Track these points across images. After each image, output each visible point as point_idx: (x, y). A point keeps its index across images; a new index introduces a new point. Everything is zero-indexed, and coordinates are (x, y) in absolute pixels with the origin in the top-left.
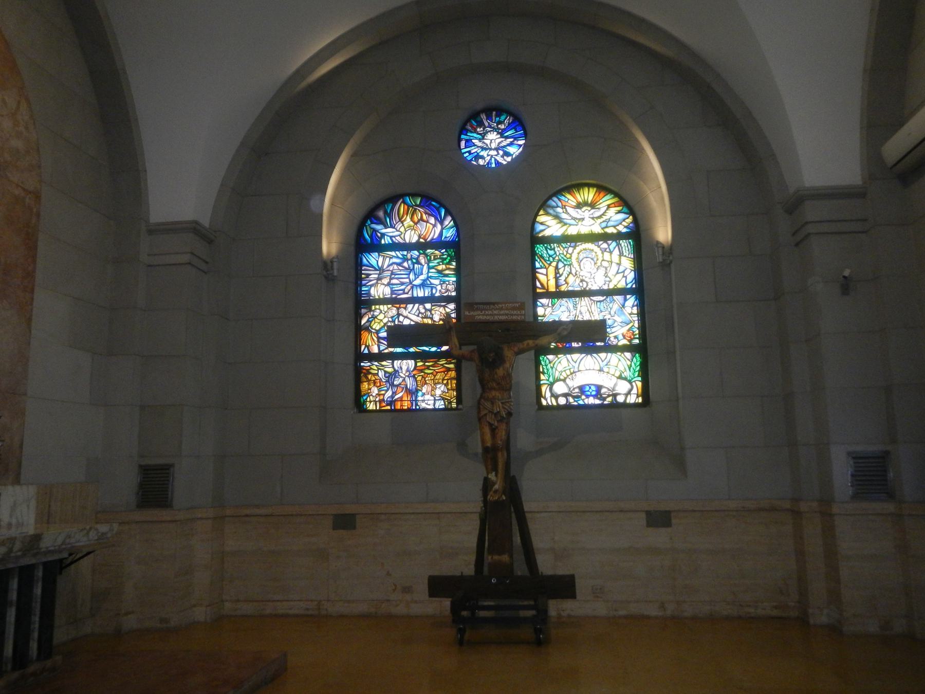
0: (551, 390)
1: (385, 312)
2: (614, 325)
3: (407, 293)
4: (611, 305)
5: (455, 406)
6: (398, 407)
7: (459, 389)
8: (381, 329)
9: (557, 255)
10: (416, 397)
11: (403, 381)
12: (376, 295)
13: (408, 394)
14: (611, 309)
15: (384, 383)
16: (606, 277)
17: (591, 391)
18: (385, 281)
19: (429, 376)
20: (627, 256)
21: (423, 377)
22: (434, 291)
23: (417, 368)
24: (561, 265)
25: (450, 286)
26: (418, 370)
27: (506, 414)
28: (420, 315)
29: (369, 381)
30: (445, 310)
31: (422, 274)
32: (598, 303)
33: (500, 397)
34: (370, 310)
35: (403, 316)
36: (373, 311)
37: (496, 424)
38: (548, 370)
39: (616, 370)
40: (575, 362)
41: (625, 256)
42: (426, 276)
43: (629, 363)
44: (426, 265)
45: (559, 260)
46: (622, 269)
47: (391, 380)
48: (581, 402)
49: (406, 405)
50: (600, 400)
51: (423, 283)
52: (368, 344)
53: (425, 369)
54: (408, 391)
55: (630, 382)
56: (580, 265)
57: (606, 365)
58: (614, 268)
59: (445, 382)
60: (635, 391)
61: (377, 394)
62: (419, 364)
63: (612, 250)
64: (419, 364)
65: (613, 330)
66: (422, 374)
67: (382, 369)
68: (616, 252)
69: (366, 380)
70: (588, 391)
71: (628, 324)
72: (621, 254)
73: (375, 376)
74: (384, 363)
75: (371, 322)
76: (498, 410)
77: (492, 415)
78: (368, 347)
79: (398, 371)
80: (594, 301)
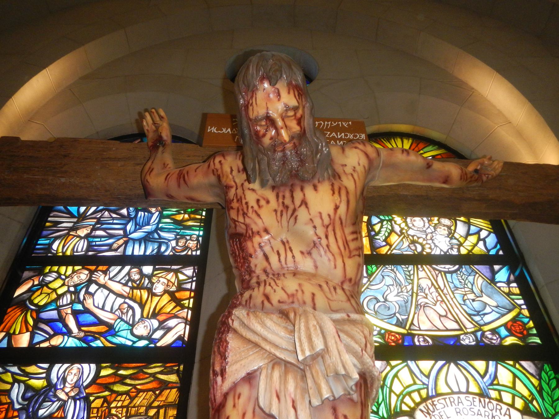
2: (485, 311)
3: (116, 250)
4: (471, 278)
8: (46, 305)
14: (472, 285)
16: (451, 238)
18: (82, 232)
19: (119, 398)
21: (105, 399)
22: (163, 248)
23: (98, 381)
25: (192, 242)
26: (99, 384)
28: (130, 284)
30: (177, 277)
31: (148, 224)
32: (449, 276)
33: (320, 301)
35: (97, 284)
36: (46, 275)
40: (428, 377)
42: (154, 227)
46: (473, 229)
47: (33, 407)
51: (146, 236)
53: (114, 383)
62: (104, 373)
64: (104, 373)
65: (487, 319)
66: (107, 393)
67: (24, 382)
71: (510, 311)
74: (32, 369)
75: (34, 292)
76: (319, 346)
77: (284, 380)
80: (440, 272)
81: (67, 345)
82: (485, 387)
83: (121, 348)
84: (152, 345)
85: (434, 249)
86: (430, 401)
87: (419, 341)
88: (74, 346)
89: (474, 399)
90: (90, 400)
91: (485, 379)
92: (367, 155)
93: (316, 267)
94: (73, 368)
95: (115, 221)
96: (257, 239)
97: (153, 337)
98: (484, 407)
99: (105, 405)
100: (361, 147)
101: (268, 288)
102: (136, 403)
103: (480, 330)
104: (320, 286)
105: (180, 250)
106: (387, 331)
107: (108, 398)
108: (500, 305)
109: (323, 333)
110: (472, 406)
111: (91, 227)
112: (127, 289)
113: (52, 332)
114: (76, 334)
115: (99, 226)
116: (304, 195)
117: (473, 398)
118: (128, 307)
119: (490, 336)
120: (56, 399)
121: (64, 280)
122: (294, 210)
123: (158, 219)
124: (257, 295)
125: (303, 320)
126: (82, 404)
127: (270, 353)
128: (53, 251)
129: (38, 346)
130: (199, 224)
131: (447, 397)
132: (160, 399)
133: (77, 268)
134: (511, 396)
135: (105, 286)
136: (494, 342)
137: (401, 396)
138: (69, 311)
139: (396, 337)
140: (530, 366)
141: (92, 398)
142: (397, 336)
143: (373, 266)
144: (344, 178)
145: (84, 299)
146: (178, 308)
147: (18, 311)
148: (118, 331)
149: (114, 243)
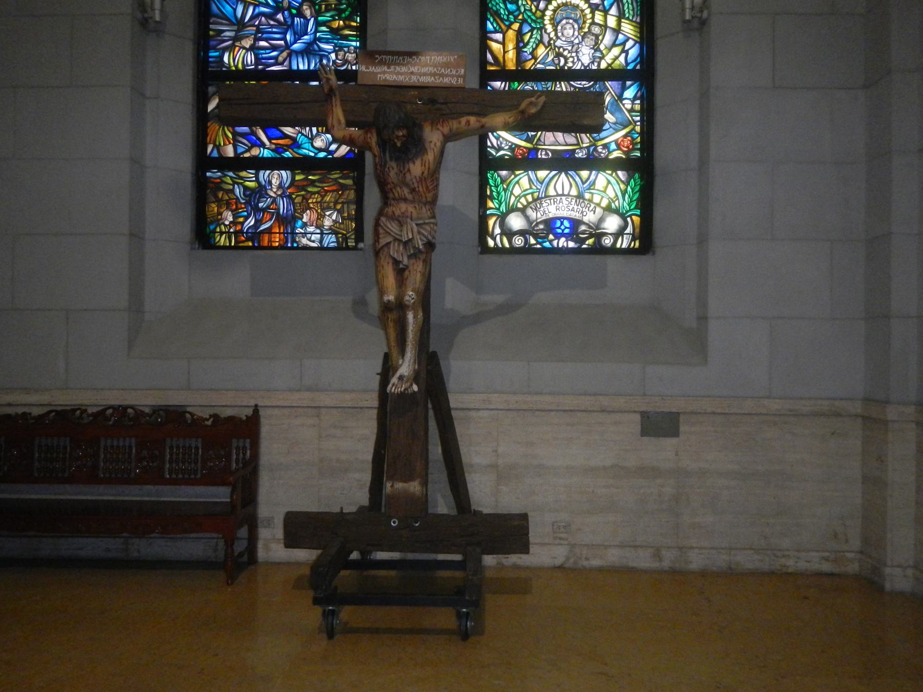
0: (503, 224)
3: (282, 64)
5: (354, 244)
6: (265, 243)
7: (359, 218)
9: (520, 13)
10: (294, 228)
11: (272, 203)
12: (232, 64)
13: (281, 223)
15: (243, 206)
16: (596, 51)
17: (563, 227)
18: (247, 43)
19: (313, 196)
20: (631, 18)
21: (304, 197)
22: (325, 62)
24: (526, 29)
25: (350, 55)
26: (296, 186)
27: (423, 244)
29: (219, 201)
31: (306, 34)
33: (415, 215)
37: (405, 261)
38: (498, 193)
39: (602, 197)
40: (542, 183)
41: (628, 19)
43: (623, 186)
44: (312, 19)
45: (524, 21)
47: (254, 202)
48: (547, 244)
49: (277, 240)
50: (576, 243)
52: (218, 144)
53: (308, 185)
54: (280, 220)
55: (623, 216)
56: (556, 30)
57: (589, 189)
58: (608, 38)
59: (339, 207)
60: (629, 230)
61: (231, 222)
62: (298, 178)
63: (607, 8)
66: (303, 193)
67: (241, 184)
68: (614, 11)
69: (214, 200)
70: (559, 228)
71: (625, 127)
72: (621, 16)
73: (230, 195)
74: (243, 174)
76: (410, 237)
77: (399, 245)
78: (217, 147)
79: (265, 187)
81: (265, 155)
82: (583, 191)
83: (306, 157)
84: (331, 157)
85: (576, 62)
86: (539, 201)
87: (541, 154)
88: (270, 156)
89: (572, 200)
91: (584, 186)
92: (443, 133)
93: (414, 199)
95: (274, 30)
96: (389, 186)
97: (330, 149)
98: (578, 206)
99: (304, 201)
100: (441, 128)
101: (394, 209)
103: (594, 145)
104: (415, 207)
105: (340, 64)
106: (517, 145)
107: (306, 197)
108: (618, 122)
109: (412, 231)
110: (569, 205)
111: (253, 36)
113: (250, 145)
115: (260, 35)
116: (409, 166)
117: (572, 199)
119: (600, 150)
120: (268, 197)
122: (405, 174)
123: (314, 27)
124: (389, 210)
125: (406, 226)
127: (394, 237)
129: (242, 156)
130: (355, 33)
131: (552, 198)
132: (343, 197)
134: (600, 197)
136: (602, 155)
137: (518, 197)
139: (523, 151)
140: (624, 175)
141: (294, 196)
142: (525, 150)
143: (516, 83)
144: (429, 153)
148: (301, 144)
149: (278, 55)
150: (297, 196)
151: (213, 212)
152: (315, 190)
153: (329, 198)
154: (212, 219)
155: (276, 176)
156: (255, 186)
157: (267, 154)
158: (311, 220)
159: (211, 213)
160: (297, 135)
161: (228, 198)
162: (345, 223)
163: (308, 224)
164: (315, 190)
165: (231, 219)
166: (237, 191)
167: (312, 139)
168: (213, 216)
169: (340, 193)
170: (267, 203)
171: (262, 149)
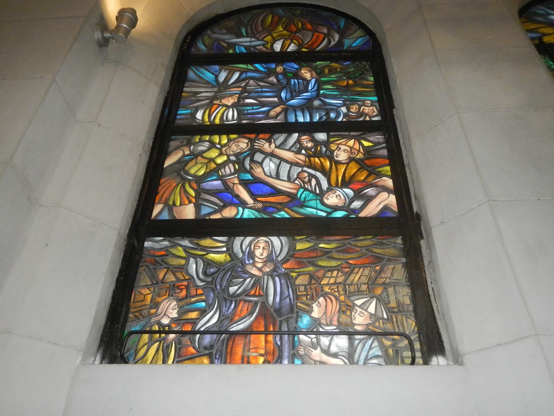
1: (223, 146)
18: (230, 101)
19: (329, 274)
21: (312, 276)
22: (332, 115)
25: (367, 108)
28: (303, 151)
29: (156, 282)
30: (361, 144)
31: (307, 91)
34: (189, 144)
35: (262, 152)
59: (379, 291)
61: (173, 320)
66: (311, 268)
74: (207, 242)
75: (187, 162)
78: (170, 208)
81: (245, 216)
90: (292, 276)
94: (260, 241)
102: (353, 280)
105: (355, 117)
111: (238, 95)
112: (302, 158)
113: (222, 204)
114: (253, 205)
118: (309, 176)
120: (247, 275)
121: (220, 149)
126: (282, 281)
128: (198, 121)
129: (208, 218)
132: (383, 275)
133: (233, 136)
135: (272, 155)
138: (236, 181)
141: (294, 275)
145: (251, 168)
146: (373, 176)
147: (173, 182)
150: (300, 274)
151: (143, 303)
152: (333, 263)
153: (357, 277)
154: (137, 314)
155: (262, 245)
156: (225, 261)
157: (248, 215)
158: (329, 315)
159: (140, 304)
160: (298, 190)
161: (175, 280)
162: (394, 319)
163: (323, 321)
164: (333, 263)
165: (174, 314)
166: (192, 268)
167: (321, 195)
168: (141, 310)
169: (378, 268)
170: (245, 285)
171: (241, 209)
